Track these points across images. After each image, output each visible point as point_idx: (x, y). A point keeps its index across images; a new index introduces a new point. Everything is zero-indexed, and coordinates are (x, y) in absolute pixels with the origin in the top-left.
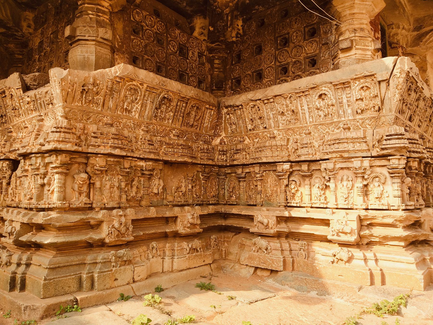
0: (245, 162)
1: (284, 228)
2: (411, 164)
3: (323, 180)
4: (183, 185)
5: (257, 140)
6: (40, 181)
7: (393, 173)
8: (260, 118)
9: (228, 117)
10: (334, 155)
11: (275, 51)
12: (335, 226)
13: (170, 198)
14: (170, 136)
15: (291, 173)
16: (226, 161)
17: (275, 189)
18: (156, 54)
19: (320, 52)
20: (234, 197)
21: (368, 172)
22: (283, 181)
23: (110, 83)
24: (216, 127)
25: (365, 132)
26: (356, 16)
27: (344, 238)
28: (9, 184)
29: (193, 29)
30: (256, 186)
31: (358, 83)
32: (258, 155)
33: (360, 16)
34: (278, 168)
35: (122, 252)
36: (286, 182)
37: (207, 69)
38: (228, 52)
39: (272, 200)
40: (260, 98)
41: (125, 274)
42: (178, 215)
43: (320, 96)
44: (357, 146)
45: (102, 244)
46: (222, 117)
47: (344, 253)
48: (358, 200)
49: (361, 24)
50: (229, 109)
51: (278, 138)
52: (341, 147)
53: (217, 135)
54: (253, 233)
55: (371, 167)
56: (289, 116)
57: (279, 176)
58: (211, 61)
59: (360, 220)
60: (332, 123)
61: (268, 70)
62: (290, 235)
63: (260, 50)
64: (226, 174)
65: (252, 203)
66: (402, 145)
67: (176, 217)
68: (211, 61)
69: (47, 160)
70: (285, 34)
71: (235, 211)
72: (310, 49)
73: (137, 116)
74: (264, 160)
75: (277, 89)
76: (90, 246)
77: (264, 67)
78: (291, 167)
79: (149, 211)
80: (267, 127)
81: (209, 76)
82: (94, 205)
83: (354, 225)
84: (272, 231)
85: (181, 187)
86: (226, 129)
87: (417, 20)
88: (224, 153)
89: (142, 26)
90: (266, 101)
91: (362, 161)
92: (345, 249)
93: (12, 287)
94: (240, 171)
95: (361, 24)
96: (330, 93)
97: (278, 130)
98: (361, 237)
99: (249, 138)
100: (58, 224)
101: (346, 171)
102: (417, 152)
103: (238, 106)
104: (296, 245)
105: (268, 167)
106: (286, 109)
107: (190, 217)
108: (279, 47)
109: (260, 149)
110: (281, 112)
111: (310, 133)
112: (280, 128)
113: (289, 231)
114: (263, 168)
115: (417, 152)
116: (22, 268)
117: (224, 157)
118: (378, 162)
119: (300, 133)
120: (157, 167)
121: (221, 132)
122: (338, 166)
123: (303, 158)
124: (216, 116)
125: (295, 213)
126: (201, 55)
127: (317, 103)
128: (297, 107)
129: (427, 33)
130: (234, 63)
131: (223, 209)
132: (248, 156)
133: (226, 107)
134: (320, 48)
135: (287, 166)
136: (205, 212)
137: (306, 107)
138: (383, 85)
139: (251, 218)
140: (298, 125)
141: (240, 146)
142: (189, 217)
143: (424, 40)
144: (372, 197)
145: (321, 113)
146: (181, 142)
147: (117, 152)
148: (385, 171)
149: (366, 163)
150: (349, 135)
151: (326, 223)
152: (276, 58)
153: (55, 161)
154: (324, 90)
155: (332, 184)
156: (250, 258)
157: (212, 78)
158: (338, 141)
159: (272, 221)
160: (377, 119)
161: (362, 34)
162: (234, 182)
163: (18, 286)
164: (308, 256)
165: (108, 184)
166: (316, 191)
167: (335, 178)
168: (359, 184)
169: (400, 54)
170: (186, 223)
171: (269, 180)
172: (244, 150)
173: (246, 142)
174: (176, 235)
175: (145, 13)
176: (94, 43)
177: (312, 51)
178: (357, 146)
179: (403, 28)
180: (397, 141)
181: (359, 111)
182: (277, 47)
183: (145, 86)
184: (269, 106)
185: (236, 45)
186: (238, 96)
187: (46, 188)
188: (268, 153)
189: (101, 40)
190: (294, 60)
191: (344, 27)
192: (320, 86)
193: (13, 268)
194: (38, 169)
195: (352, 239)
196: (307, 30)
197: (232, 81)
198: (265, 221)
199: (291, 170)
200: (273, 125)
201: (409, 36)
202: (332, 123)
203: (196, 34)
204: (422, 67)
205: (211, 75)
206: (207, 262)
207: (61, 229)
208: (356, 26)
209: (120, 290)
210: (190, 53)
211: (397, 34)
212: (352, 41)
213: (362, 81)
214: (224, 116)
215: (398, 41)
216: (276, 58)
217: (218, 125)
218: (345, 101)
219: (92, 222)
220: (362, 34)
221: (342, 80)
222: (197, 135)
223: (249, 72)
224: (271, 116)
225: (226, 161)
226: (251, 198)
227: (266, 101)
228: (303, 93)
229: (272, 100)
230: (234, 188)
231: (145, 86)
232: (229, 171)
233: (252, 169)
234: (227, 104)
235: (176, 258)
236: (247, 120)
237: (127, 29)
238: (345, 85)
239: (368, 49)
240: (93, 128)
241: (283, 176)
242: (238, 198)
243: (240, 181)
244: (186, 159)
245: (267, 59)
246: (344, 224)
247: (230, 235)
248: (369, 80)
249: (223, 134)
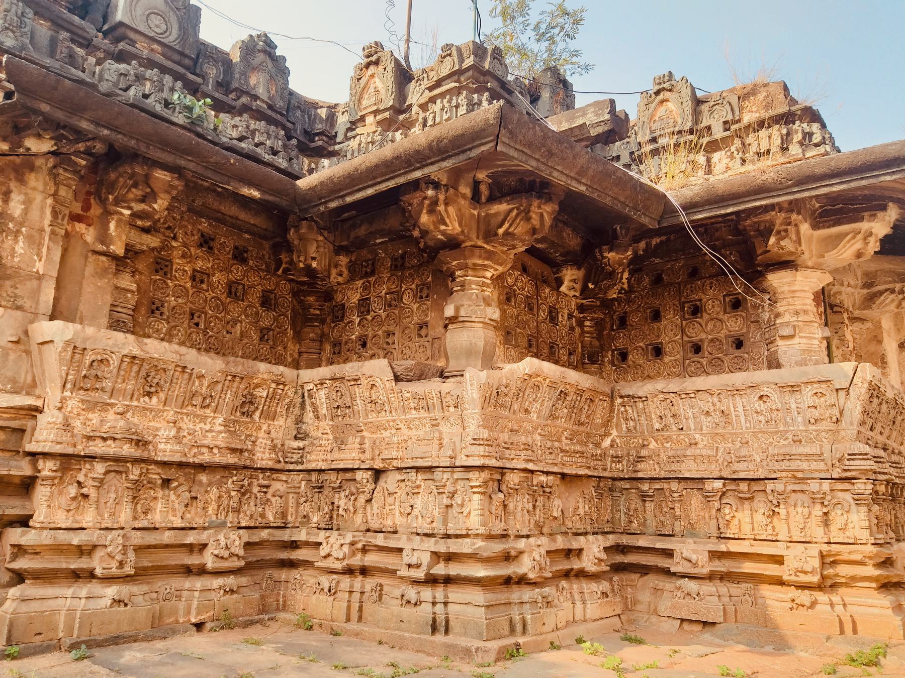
0: (653, 474)
1: (721, 566)
3: (769, 504)
5: (668, 445)
6: (446, 501)
7: (858, 499)
8: (674, 416)
9: (622, 409)
10: (784, 474)
12: (791, 563)
13: (570, 525)
15: (724, 493)
16: (623, 471)
17: (702, 514)
19: (748, 332)
20: (635, 525)
21: (828, 498)
23: (519, 382)
24: (607, 424)
25: (821, 446)
26: (797, 294)
27: (803, 578)
28: (369, 501)
29: (560, 282)
30: (674, 509)
31: (810, 387)
32: (674, 467)
34: (706, 486)
35: (546, 590)
37: (577, 335)
41: (552, 618)
43: (761, 397)
44: (814, 465)
45: (522, 581)
47: (805, 597)
48: (818, 533)
49: (804, 304)
50: (626, 399)
51: (700, 446)
52: (794, 465)
53: (607, 434)
54: (674, 574)
56: (717, 417)
57: (707, 496)
58: (580, 323)
59: (822, 556)
60: (777, 432)
62: (725, 577)
63: (656, 316)
65: (667, 533)
66: (868, 467)
67: (580, 551)
68: (580, 323)
69: (456, 476)
70: (696, 301)
71: (642, 542)
72: (734, 325)
73: (535, 418)
74: (687, 475)
75: (700, 382)
76: (508, 581)
78: (724, 485)
79: (554, 541)
80: (685, 428)
82: (510, 532)
83: (816, 563)
84: (705, 571)
86: (618, 426)
87: (866, 274)
89: (515, 291)
90: (683, 396)
91: (821, 484)
92: (807, 592)
93: (434, 629)
94: (645, 487)
95: (804, 304)
96: (775, 395)
97: (702, 434)
98: (823, 577)
99: (656, 441)
100: (485, 555)
101: (799, 495)
103: (640, 398)
104: (736, 589)
105: (690, 484)
106: (712, 408)
107: (596, 550)
108: (687, 316)
109: (676, 459)
111: (747, 443)
113: (727, 570)
114: (683, 485)
116: (439, 608)
117: (620, 466)
119: (733, 441)
122: (790, 487)
123: (742, 475)
125: (734, 547)
126: (570, 316)
127: (756, 406)
128: (728, 408)
129: (881, 293)
131: (625, 540)
132: (656, 466)
133: (622, 397)
134: (748, 327)
135: (718, 484)
136: (608, 544)
137: (740, 409)
138: (842, 394)
139: (668, 553)
140: (729, 429)
141: (644, 453)
143: (878, 302)
144: (833, 528)
145: (762, 418)
146: (578, 448)
147: (531, 466)
148: (848, 496)
149: (826, 486)
150: (801, 450)
151: (778, 560)
152: (683, 331)
153: (477, 478)
154: (765, 390)
155: (782, 510)
156: (674, 607)
157: (583, 347)
158: (789, 457)
159: (703, 558)
160: (835, 432)
161: (806, 318)
162: (636, 503)
163: (443, 629)
164: (755, 604)
165: (520, 505)
166: (759, 518)
167: (786, 503)
168: (818, 511)
169: (846, 321)
170: (591, 557)
171: (692, 502)
172: (650, 457)
173: (651, 446)
174: (582, 574)
176: (481, 325)
178: (814, 465)
179: (848, 286)
180: (863, 462)
181: (812, 421)
182: (684, 316)
183: (548, 380)
184: (687, 401)
185: (619, 304)
186: (641, 384)
187: (455, 510)
188: (691, 464)
189: (489, 322)
190: (710, 337)
191: (780, 307)
193: (426, 608)
194: (444, 486)
195: (815, 579)
196: (727, 299)
197: (613, 352)
198: (694, 557)
199: (724, 490)
200: (693, 427)
201: (856, 294)
202: (777, 432)
203: (563, 289)
204: (876, 336)
205: (582, 342)
206: (617, 612)
207: (488, 561)
208: (798, 307)
209: (551, 637)
211: (840, 293)
213: (815, 386)
217: (609, 421)
218: (793, 406)
219: (513, 553)
222: (588, 435)
223: (641, 344)
224: (691, 414)
225: (623, 471)
226: (664, 526)
228: (739, 391)
229: (692, 395)
230: (636, 510)
231: (548, 380)
232: (628, 486)
233: (666, 486)
235: (587, 603)
237: (501, 297)
238: (794, 388)
239: (814, 338)
240: (505, 436)
241: (713, 496)
242: (644, 523)
243: (645, 501)
246: (802, 561)
247: (635, 576)
248: (824, 385)
249: (614, 433)
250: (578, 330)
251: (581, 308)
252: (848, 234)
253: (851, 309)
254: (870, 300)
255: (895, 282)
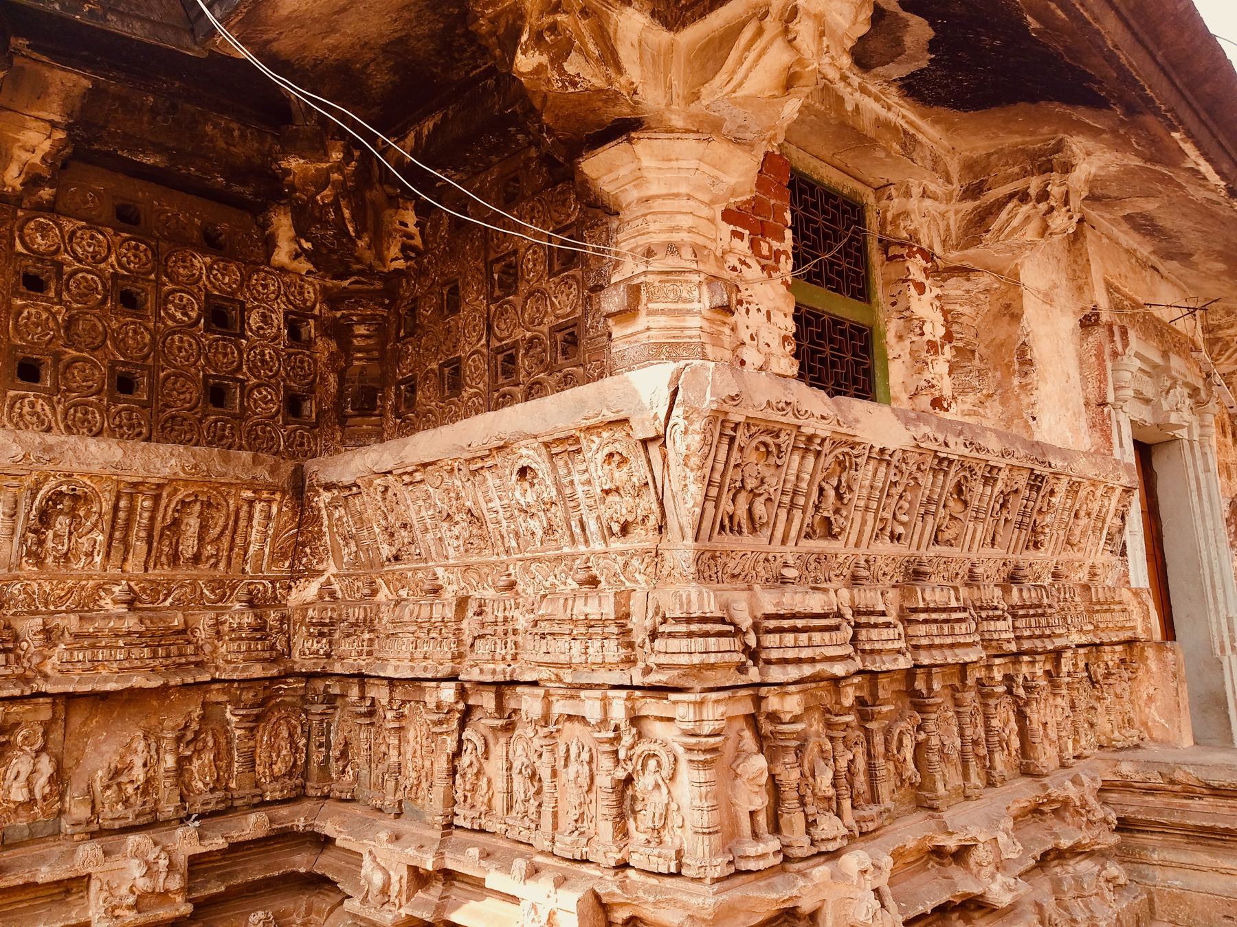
2: (773, 703)
4: (138, 761)
8: (404, 526)
11: (488, 306)
14: (102, 603)
18: (114, 340)
21: (627, 740)
22: (444, 741)
24: (298, 550)
26: (656, 205)
29: (270, 244)
33: (670, 205)
36: (451, 744)
37: (323, 357)
38: (387, 302)
39: (419, 801)
40: (389, 469)
42: (89, 870)
43: (523, 472)
46: (317, 519)
49: (672, 229)
55: (635, 720)
58: (339, 332)
60: (559, 559)
61: (474, 361)
64: (330, 700)
66: (696, 659)
68: (339, 332)
70: (509, 255)
72: (564, 302)
75: (426, 444)
77: (464, 351)
78: (462, 693)
81: (332, 379)
85: (130, 767)
86: (336, 552)
87: (969, 167)
88: (324, 630)
89: (59, 265)
95: (672, 229)
96: (541, 466)
102: (799, 661)
103: (349, 488)
108: (497, 293)
110: (445, 515)
111: (511, 586)
112: (451, 561)
115: (799, 661)
118: (651, 707)
120: (30, 717)
121: (321, 561)
124: (293, 519)
127: (518, 494)
129: (1000, 204)
130: (402, 334)
138: (654, 450)
142: (135, 870)
143: (994, 227)
145: (534, 524)
157: (342, 381)
161: (671, 262)
170: (124, 890)
175: (68, 225)
177: (569, 310)
179: (925, 194)
180: (683, 644)
181: (616, 528)
182: (492, 293)
190: (528, 334)
191: (627, 242)
192: (516, 445)
197: (398, 388)
201: (951, 214)
203: (282, 255)
204: (1008, 306)
208: (657, 239)
210: (254, 320)
211: (905, 214)
212: (634, 291)
214: (324, 512)
215: (914, 235)
216: (490, 328)
217: (304, 545)
220: (671, 262)
221: (556, 429)
223: (434, 366)
227: (407, 478)
228: (478, 464)
234: (324, 478)
236: (377, 530)
239: (689, 312)
244: (138, 681)
245: (471, 329)
249: (331, 569)
250: (324, 348)
251: (333, 299)
252: (742, 25)
253: (938, 250)
254: (979, 222)
255: (1025, 173)
